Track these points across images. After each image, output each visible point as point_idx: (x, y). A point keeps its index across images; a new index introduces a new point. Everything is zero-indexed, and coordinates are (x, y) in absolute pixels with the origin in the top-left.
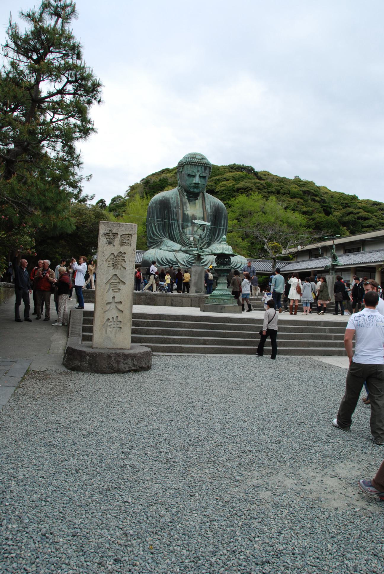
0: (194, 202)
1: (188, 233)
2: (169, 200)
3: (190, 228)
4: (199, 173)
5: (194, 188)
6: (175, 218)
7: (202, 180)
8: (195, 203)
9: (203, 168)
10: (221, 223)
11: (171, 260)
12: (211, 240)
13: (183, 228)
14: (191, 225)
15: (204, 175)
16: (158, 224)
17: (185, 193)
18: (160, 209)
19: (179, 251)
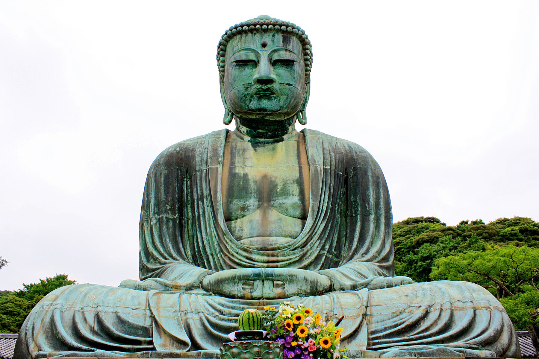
0: (270, 146)
1: (246, 232)
2: (193, 150)
3: (255, 216)
4: (269, 50)
5: (260, 98)
6: (206, 193)
7: (282, 71)
8: (274, 149)
9: (279, 37)
10: (365, 200)
11: (121, 321)
12: (338, 256)
13: (228, 219)
14: (259, 207)
15: (285, 55)
16: (160, 221)
17: (244, 129)
18: (167, 177)
19: (190, 288)
